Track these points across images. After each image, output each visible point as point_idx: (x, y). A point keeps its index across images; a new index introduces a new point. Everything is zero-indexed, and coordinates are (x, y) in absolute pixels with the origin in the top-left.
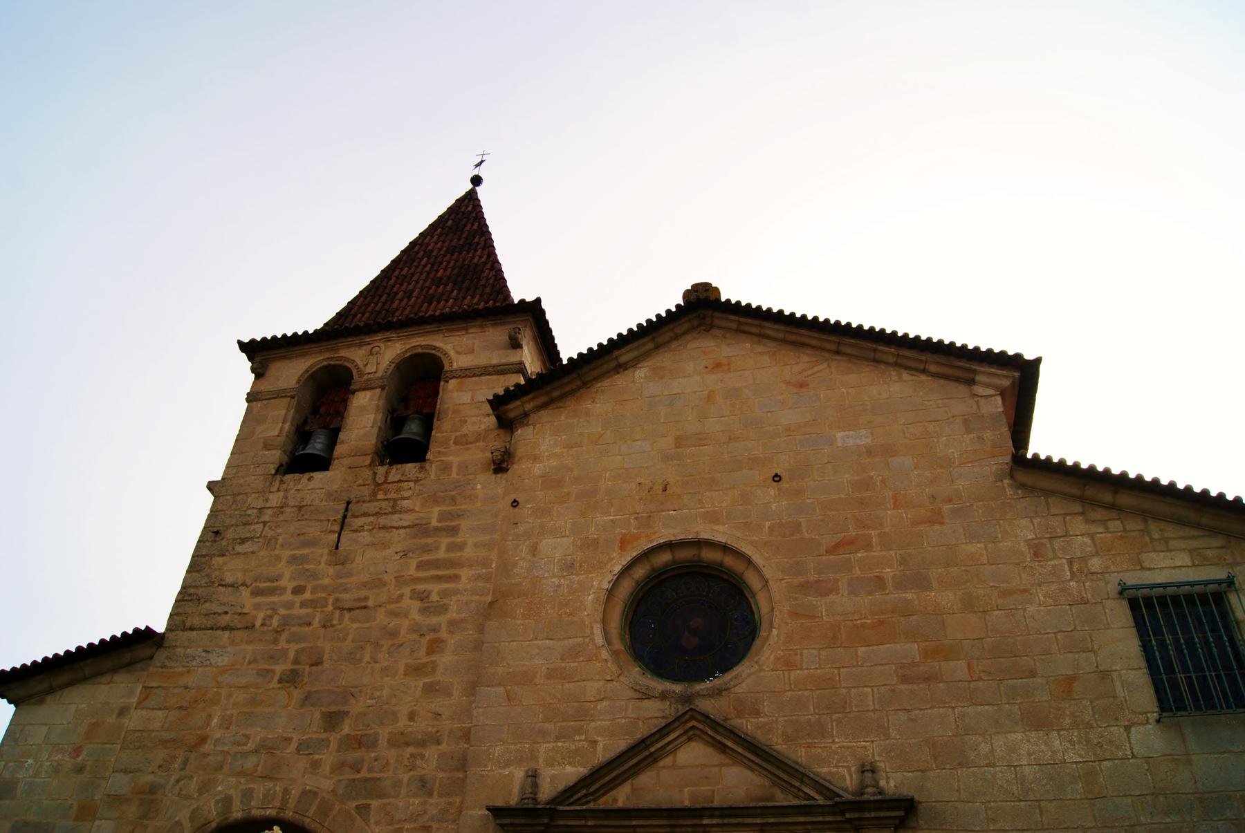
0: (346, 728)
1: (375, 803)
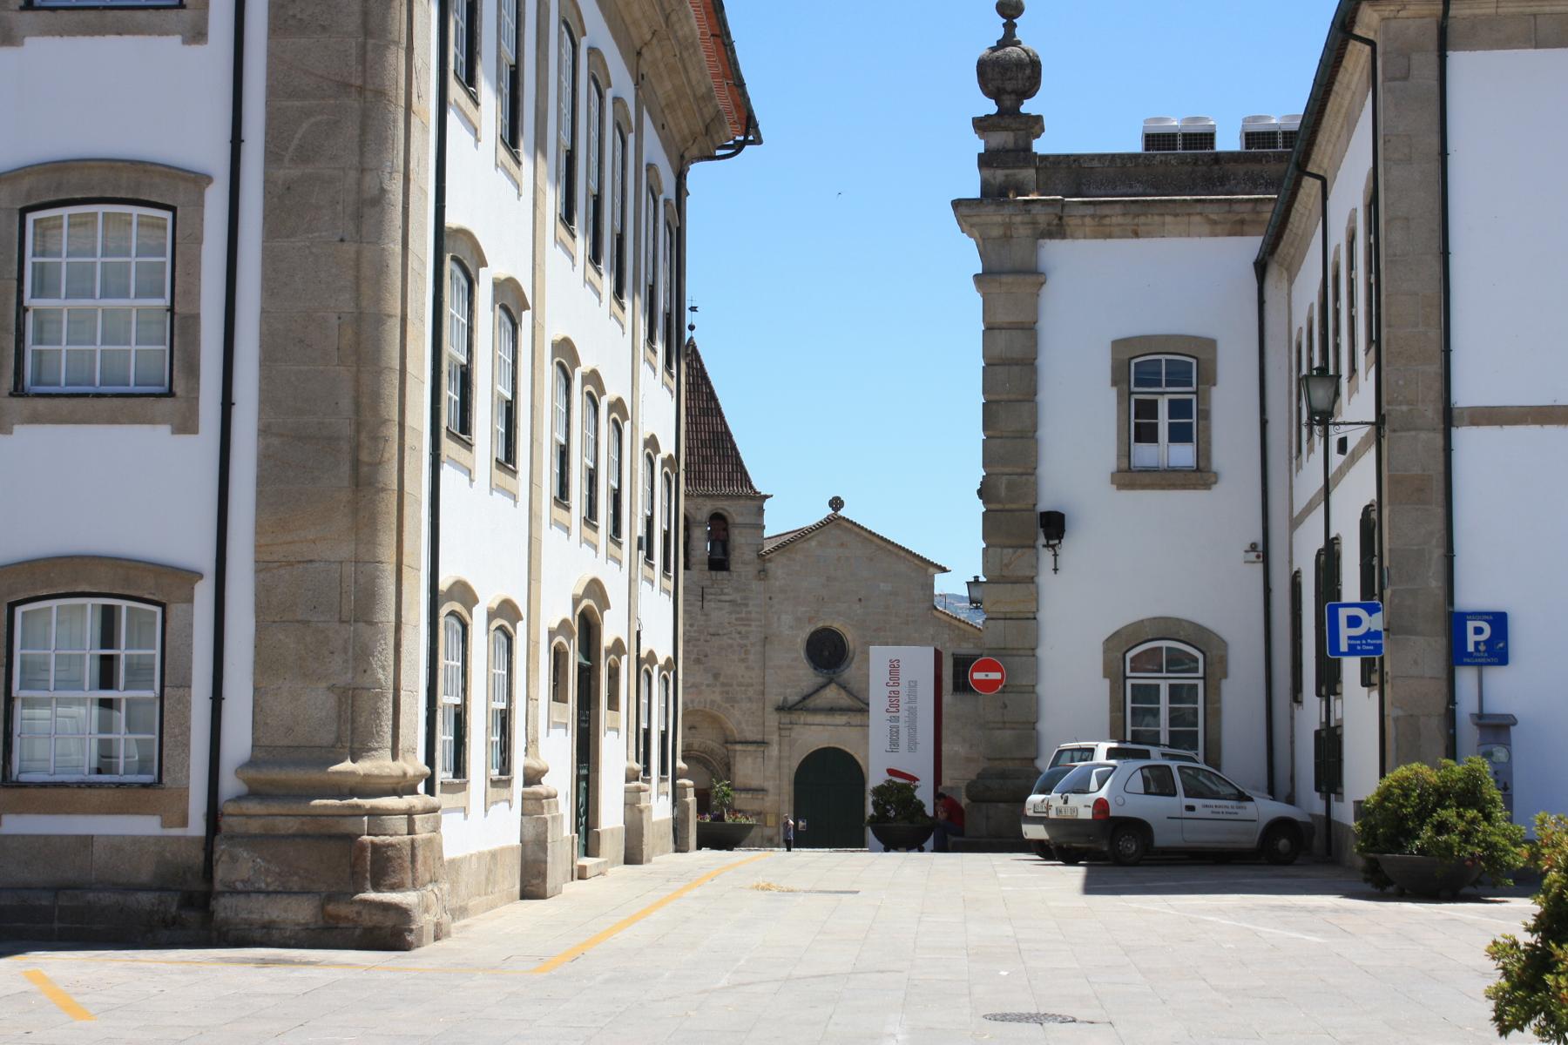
0: (722, 679)
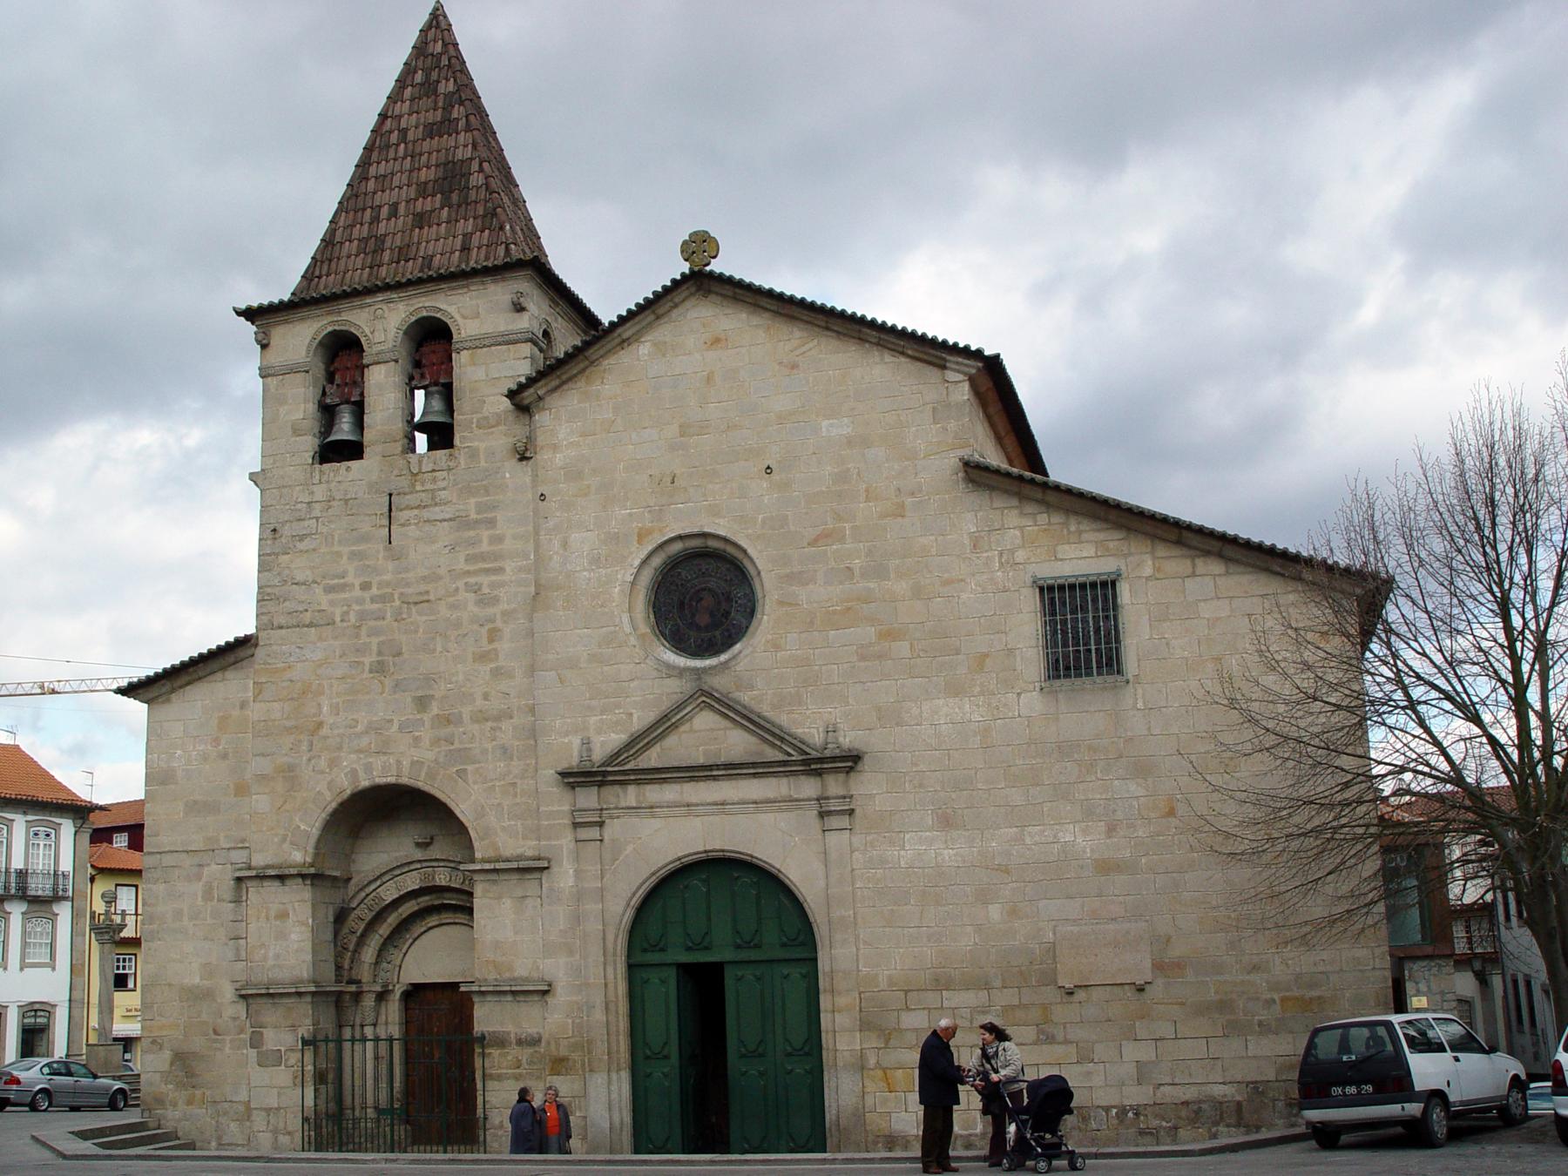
0: (435, 709)
1: (470, 768)
